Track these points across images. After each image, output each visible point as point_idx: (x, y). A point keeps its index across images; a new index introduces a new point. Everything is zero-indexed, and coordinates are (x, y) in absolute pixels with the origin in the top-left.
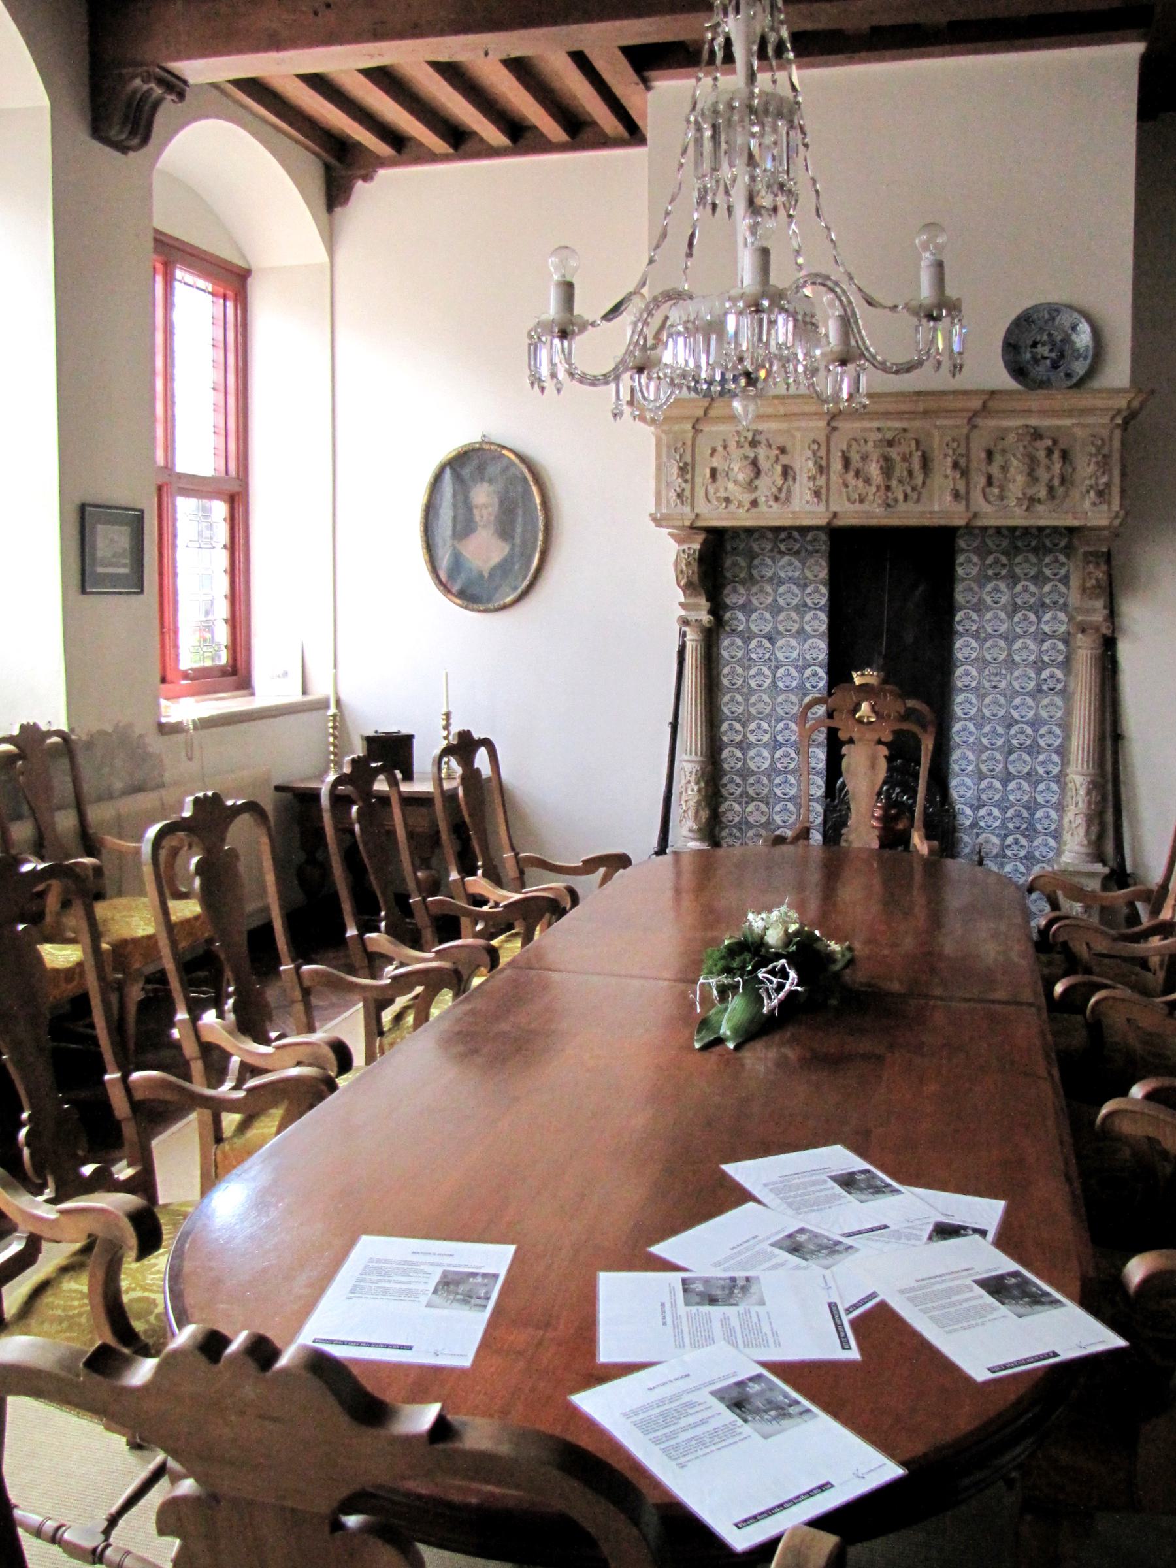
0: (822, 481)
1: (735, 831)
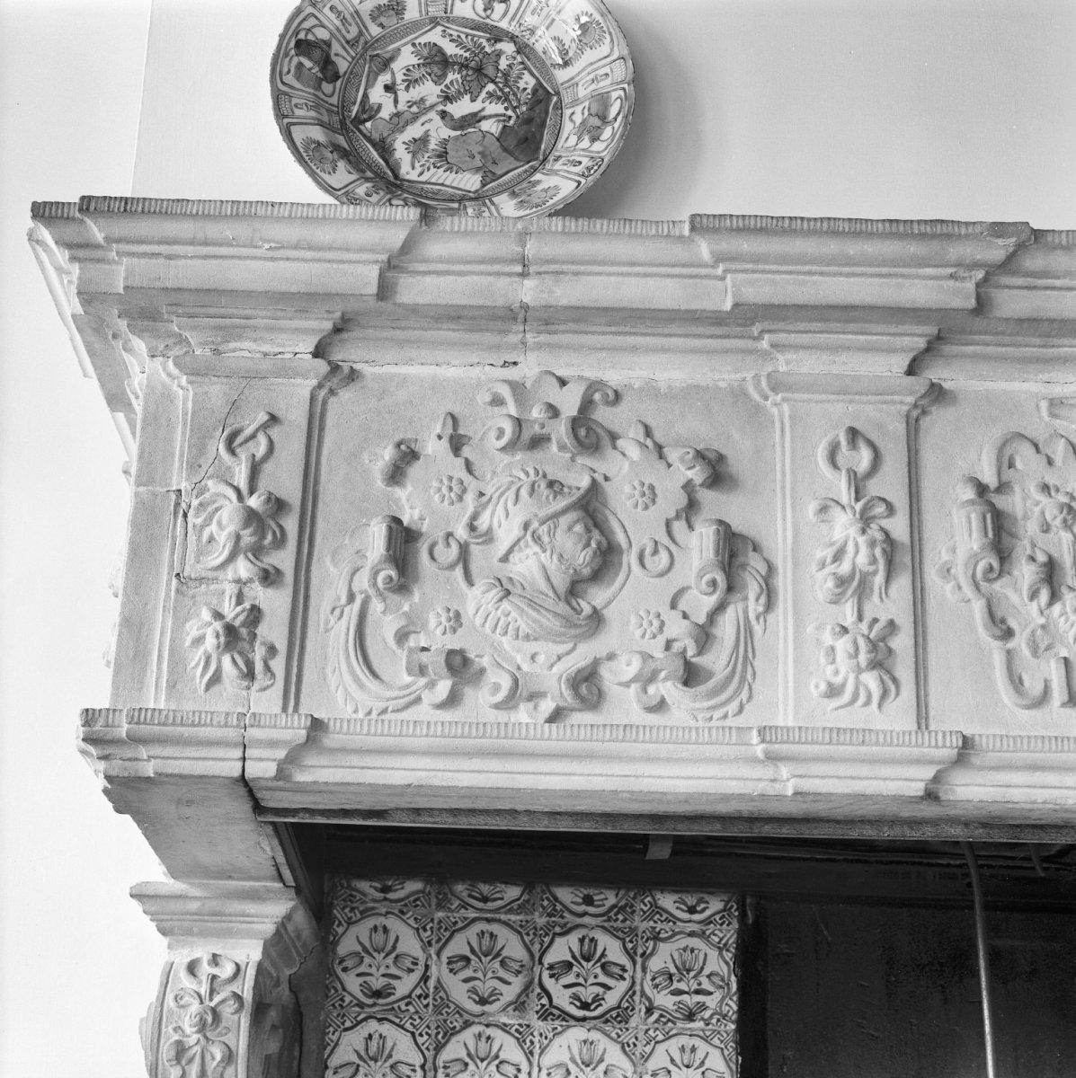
0: (893, 604)
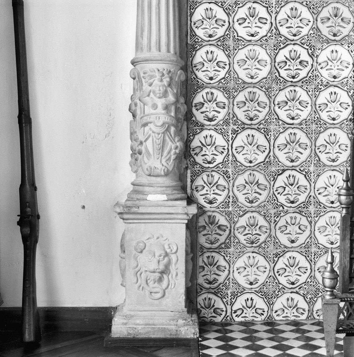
1: (216, 176)
